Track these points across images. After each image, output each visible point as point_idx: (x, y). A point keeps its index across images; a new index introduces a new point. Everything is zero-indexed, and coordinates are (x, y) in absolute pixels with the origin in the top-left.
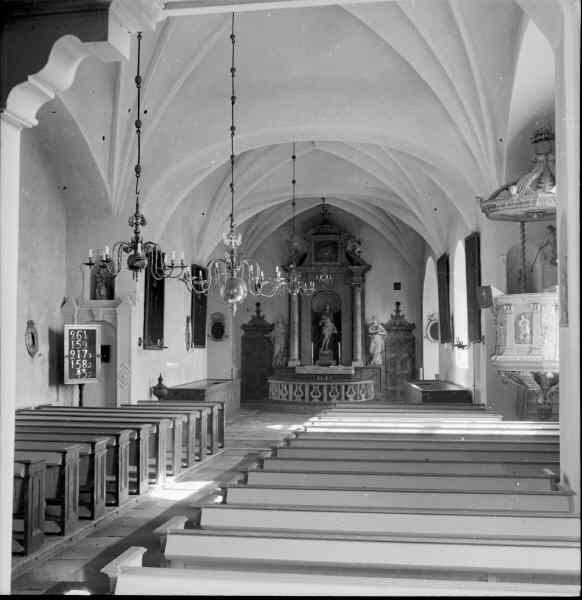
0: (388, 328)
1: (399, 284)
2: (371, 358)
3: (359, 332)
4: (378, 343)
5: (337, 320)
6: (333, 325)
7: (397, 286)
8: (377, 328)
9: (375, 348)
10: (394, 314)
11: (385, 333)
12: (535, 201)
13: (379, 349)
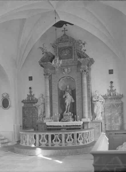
0: (105, 98)
1: (112, 70)
2: (96, 117)
3: (86, 100)
4: (99, 108)
5: (73, 94)
6: (71, 96)
7: (111, 72)
8: (98, 97)
9: (97, 109)
10: (110, 89)
11: (103, 100)
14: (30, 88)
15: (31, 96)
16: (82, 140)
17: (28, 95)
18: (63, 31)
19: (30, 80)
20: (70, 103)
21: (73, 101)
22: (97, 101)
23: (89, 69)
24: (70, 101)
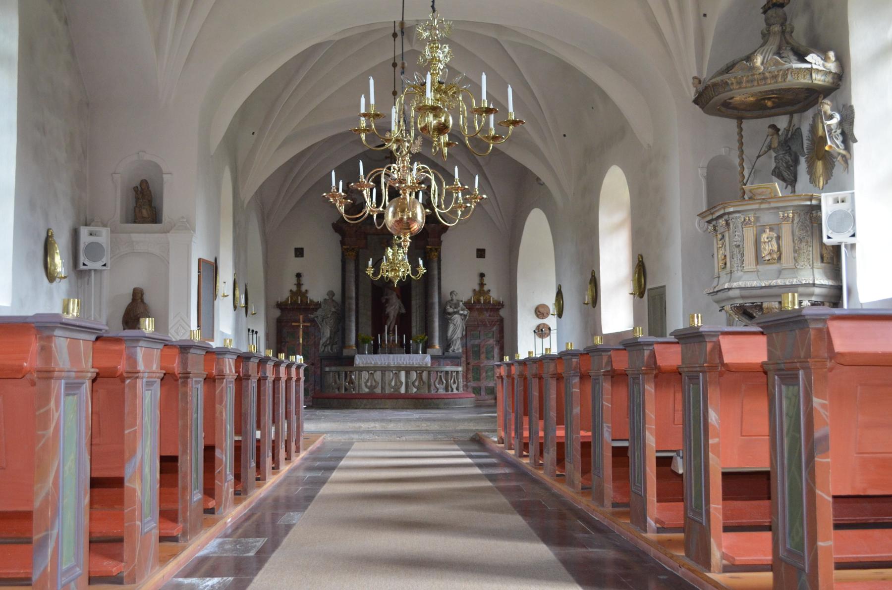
2: (449, 346)
7: (481, 253)
8: (456, 306)
9: (454, 332)
10: (477, 288)
12: (785, 76)
13: (459, 334)
14: (299, 276)
15: (299, 292)
16: (444, 385)
17: (291, 291)
18: (388, 157)
19: (296, 256)
20: (396, 316)
21: (403, 311)
22: (455, 313)
23: (440, 243)
24: (397, 312)
